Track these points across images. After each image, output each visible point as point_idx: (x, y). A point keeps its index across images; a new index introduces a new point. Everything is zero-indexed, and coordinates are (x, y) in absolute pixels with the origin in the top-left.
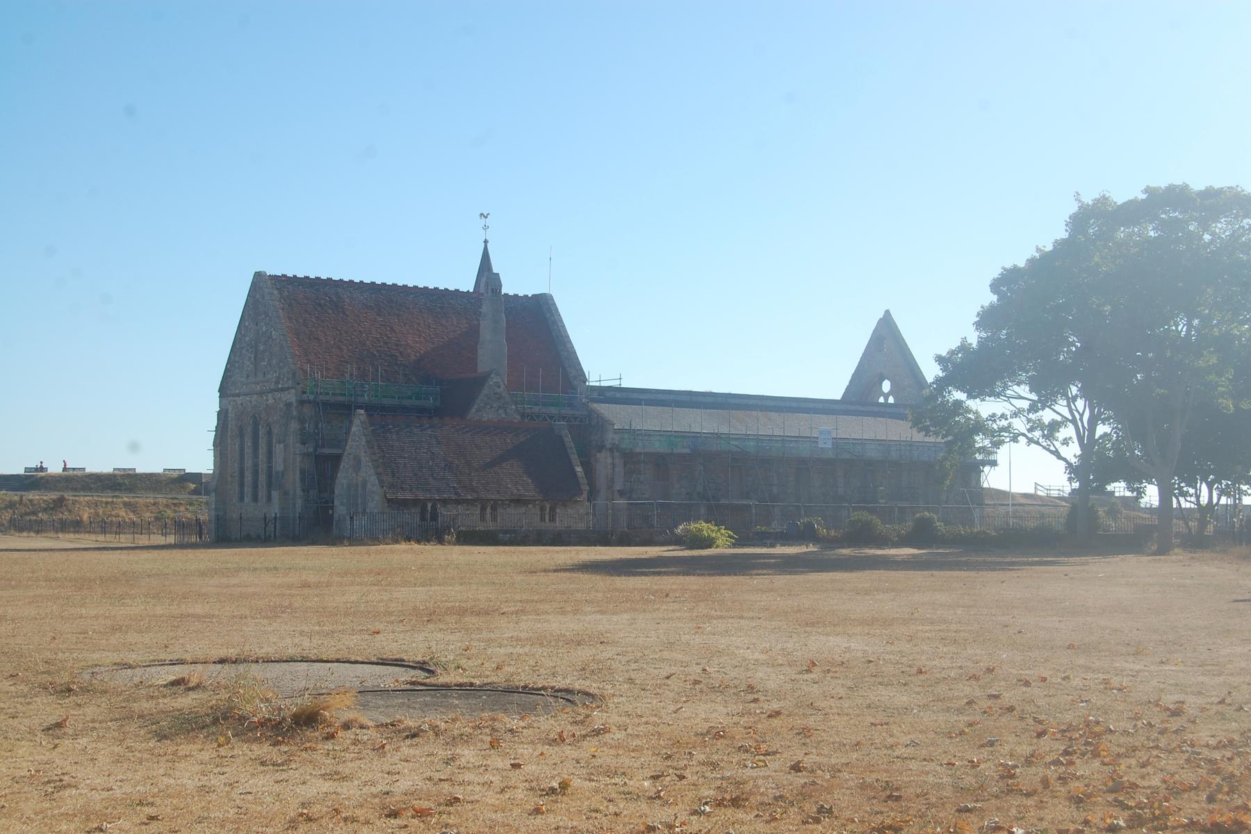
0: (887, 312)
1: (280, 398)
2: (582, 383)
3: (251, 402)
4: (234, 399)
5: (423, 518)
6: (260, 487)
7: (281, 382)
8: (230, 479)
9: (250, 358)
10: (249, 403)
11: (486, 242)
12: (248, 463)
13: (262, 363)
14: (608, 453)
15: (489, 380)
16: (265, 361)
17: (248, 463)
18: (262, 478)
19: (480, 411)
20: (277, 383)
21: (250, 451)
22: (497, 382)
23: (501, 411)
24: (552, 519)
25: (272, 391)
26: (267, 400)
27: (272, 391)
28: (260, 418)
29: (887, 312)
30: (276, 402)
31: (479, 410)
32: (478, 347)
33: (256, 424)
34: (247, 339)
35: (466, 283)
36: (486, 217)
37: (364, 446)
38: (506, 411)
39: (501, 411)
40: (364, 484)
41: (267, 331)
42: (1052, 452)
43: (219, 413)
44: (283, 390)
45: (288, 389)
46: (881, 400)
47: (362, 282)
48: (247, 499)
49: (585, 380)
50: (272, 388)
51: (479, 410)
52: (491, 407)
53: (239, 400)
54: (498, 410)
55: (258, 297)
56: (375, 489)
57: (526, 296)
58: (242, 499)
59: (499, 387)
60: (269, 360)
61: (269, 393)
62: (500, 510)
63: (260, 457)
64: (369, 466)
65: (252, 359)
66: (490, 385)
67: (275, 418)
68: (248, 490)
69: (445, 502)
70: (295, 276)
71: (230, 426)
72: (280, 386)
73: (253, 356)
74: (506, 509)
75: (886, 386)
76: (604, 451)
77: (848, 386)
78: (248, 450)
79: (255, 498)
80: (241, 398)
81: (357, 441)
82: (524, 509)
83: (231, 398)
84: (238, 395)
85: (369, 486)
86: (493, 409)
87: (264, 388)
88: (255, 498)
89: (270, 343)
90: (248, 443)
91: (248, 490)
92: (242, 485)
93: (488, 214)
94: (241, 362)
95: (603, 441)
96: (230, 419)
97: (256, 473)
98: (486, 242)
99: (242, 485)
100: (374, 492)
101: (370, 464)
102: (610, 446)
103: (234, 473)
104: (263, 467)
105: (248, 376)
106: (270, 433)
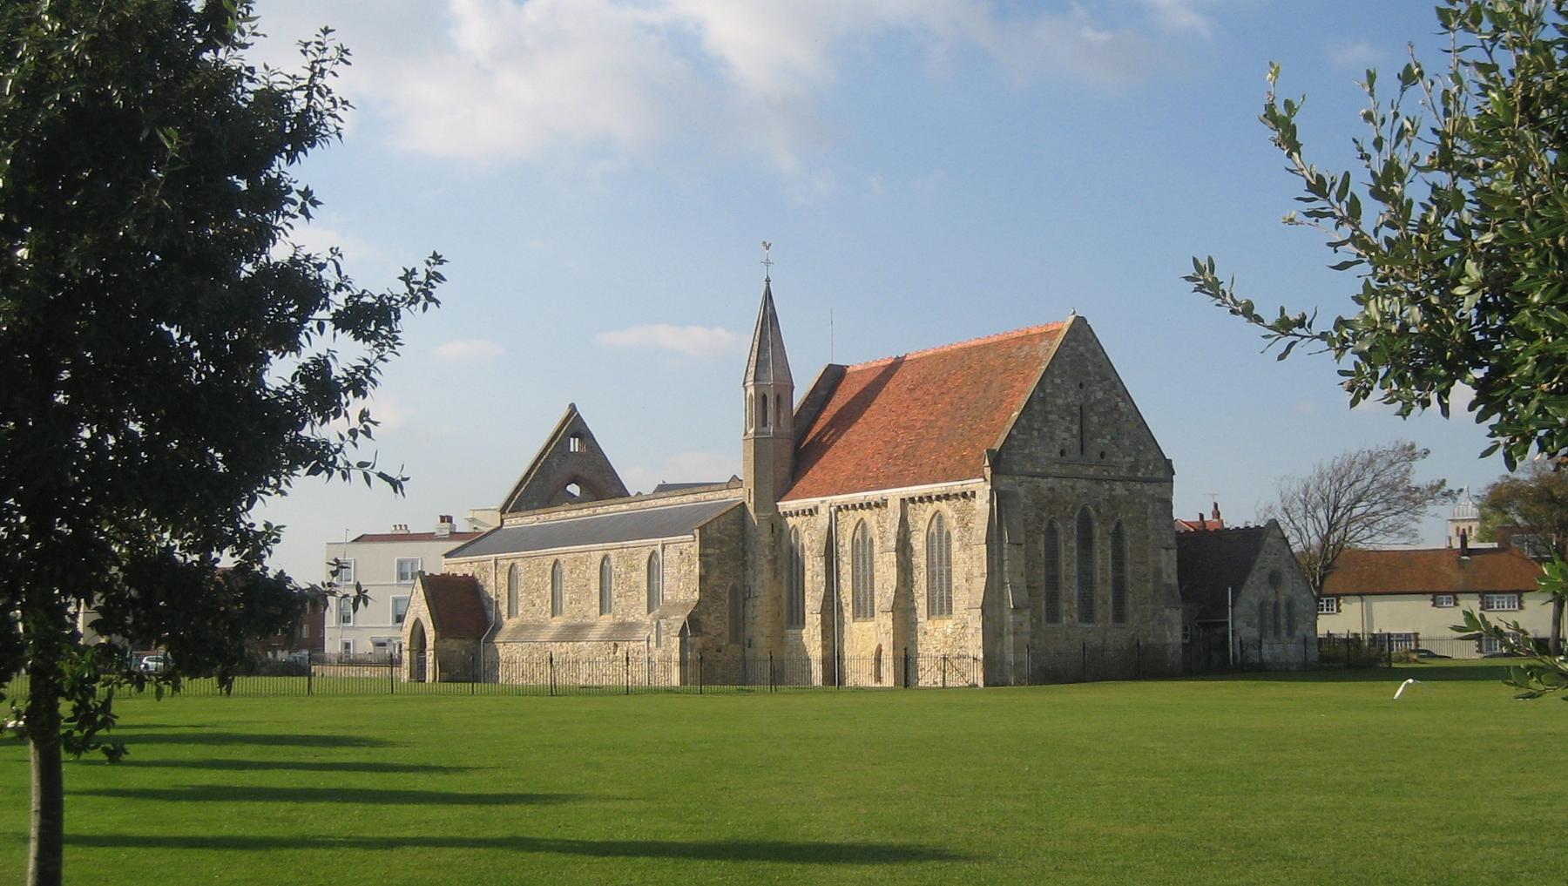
0: (573, 408)
3: (1073, 488)
4: (1030, 479)
7: (1143, 470)
10: (1070, 490)
11: (768, 281)
13: (1099, 440)
16: (1103, 437)
18: (1104, 592)
20: (1134, 467)
25: (1122, 479)
26: (1111, 489)
27: (1122, 479)
29: (573, 408)
40: (1290, 604)
50: (1122, 474)
53: (1044, 484)
61: (1116, 481)
65: (1075, 432)
67: (1130, 515)
72: (1140, 475)
73: (1075, 428)
80: (1050, 480)
83: (1023, 478)
84: (1044, 476)
87: (1105, 473)
88: (1087, 614)
94: (1045, 430)
97: (1086, 581)
98: (768, 281)
99: (1053, 598)
100: (1307, 612)
105: (1062, 453)
106: (1118, 535)
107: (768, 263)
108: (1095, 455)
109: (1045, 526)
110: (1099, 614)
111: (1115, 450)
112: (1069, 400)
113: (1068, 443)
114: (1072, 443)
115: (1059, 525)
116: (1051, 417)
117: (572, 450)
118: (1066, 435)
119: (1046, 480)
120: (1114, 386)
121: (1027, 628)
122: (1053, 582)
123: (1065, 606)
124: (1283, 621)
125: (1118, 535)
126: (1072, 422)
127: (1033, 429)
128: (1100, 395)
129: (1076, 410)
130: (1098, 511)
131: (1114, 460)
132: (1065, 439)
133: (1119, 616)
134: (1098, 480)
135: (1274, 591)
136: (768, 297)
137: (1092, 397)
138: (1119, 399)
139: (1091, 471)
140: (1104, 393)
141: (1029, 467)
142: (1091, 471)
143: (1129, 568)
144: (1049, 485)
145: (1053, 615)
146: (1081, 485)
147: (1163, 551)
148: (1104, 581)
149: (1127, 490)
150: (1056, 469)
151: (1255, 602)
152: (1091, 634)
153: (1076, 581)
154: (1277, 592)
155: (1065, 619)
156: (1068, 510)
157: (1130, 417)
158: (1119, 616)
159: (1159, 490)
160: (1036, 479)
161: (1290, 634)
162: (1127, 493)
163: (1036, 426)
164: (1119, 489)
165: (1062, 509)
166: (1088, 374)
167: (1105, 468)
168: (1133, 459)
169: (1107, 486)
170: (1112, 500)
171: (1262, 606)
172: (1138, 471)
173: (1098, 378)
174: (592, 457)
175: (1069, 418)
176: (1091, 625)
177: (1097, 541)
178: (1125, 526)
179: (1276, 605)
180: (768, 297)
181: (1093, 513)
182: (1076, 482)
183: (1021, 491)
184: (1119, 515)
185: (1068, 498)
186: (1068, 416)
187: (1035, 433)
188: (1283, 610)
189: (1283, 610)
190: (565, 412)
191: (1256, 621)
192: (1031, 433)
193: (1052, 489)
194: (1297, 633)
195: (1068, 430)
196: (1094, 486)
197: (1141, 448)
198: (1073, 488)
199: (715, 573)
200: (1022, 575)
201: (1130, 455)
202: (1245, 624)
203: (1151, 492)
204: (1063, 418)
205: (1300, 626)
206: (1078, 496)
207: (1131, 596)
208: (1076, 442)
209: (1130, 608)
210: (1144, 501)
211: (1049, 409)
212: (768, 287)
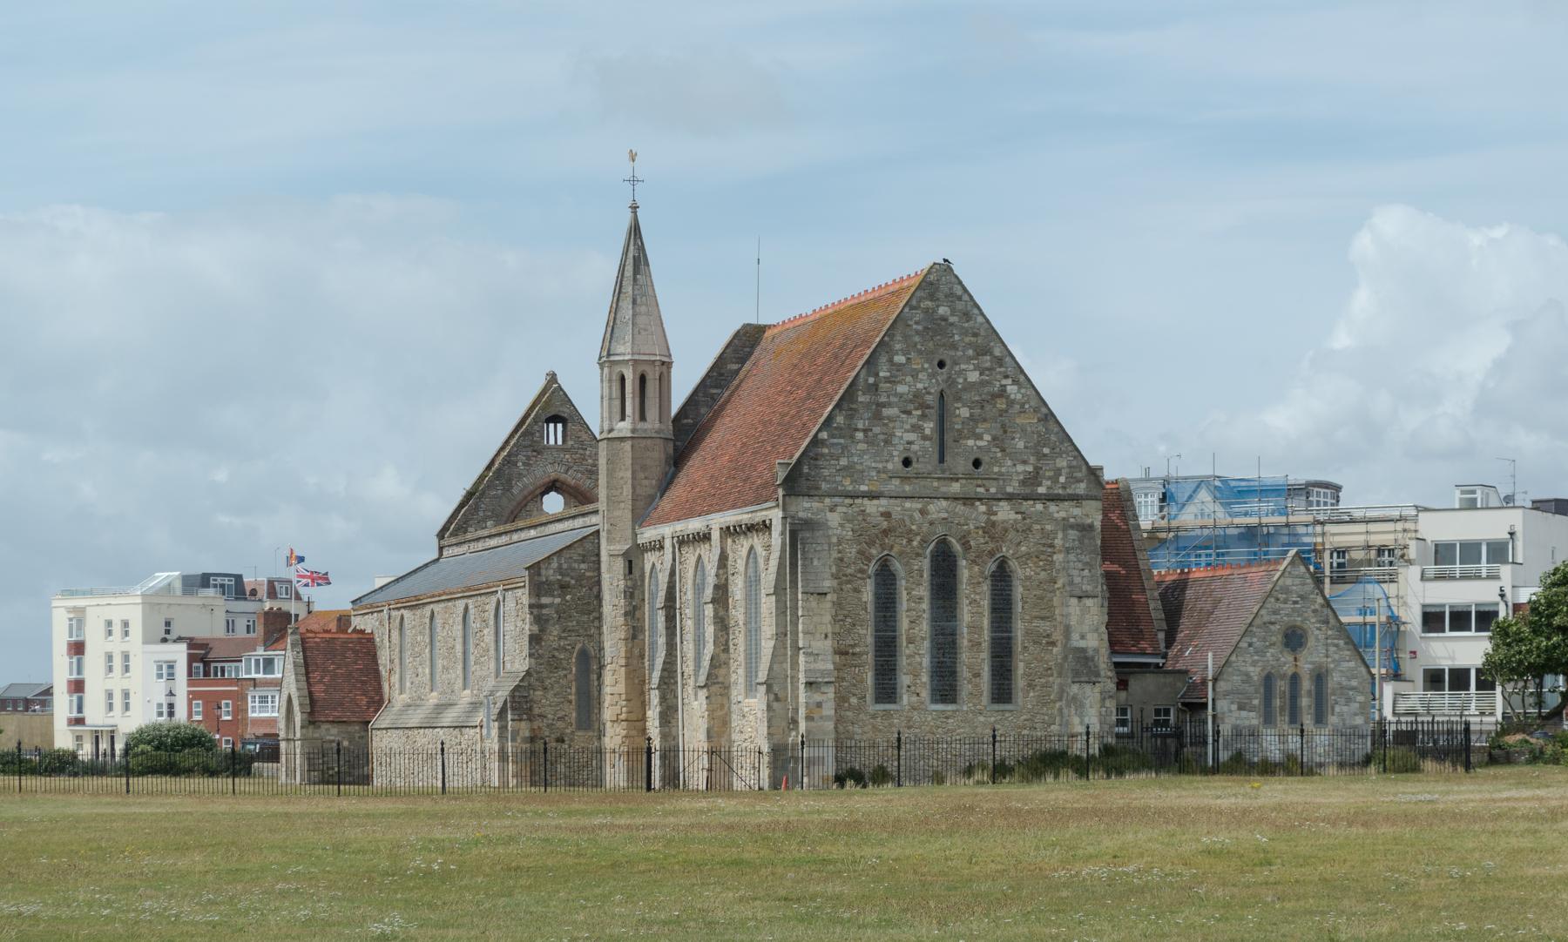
0: (552, 378)
4: (848, 501)
10: (917, 515)
11: (634, 208)
13: (970, 442)
16: (979, 437)
18: (974, 661)
20: (1033, 479)
21: (925, 605)
25: (1010, 498)
26: (991, 512)
28: (966, 546)
29: (552, 378)
30: (1024, 519)
34: (901, 389)
37: (1315, 611)
40: (1320, 678)
45: (1076, 498)
50: (1009, 490)
53: (872, 507)
56: (1354, 683)
60: (994, 438)
61: (1000, 500)
64: (1336, 646)
65: (928, 432)
72: (1041, 490)
73: (929, 427)
80: (883, 501)
81: (1295, 602)
83: (837, 500)
84: (873, 496)
85: (1335, 679)
98: (634, 208)
100: (1353, 688)
103: (853, 646)
105: (907, 462)
106: (1001, 578)
107: (634, 181)
108: (962, 465)
109: (872, 569)
110: (965, 688)
111: (999, 455)
112: (920, 386)
113: (915, 447)
114: (924, 448)
115: (897, 566)
116: (886, 412)
117: (552, 442)
118: (912, 436)
119: (875, 502)
120: (1000, 361)
121: (829, 710)
122: (886, 648)
123: (904, 680)
124: (1305, 702)
125: (1001, 578)
126: (923, 417)
127: (857, 430)
128: (974, 377)
129: (931, 399)
130: (966, 546)
131: (996, 469)
132: (909, 443)
133: (1002, 692)
134: (968, 500)
135: (1291, 659)
136: (635, 231)
137: (961, 380)
138: (1009, 381)
139: (955, 487)
140: (981, 375)
141: (848, 485)
142: (955, 487)
143: (1019, 628)
144: (881, 509)
145: (886, 691)
146: (938, 509)
147: (1074, 601)
148: (976, 645)
149: (1017, 513)
151: (1255, 672)
152: (950, 721)
153: (927, 644)
154: (1296, 659)
155: (905, 699)
156: (915, 543)
157: (1027, 406)
158: (1002, 692)
159: (1077, 511)
160: (858, 501)
161: (1320, 719)
162: (1019, 517)
163: (860, 426)
164: (1005, 512)
165: (904, 542)
166: (954, 347)
167: (979, 482)
168: (1030, 468)
169: (983, 508)
170: (990, 529)
171: (1268, 680)
172: (1040, 484)
173: (970, 352)
174: (581, 451)
175: (919, 412)
176: (950, 707)
177: (964, 587)
178: (1013, 564)
179: (1295, 679)
180: (635, 231)
181: (957, 547)
182: (929, 503)
183: (834, 519)
184: (1004, 549)
185: (914, 527)
186: (916, 409)
187: (860, 435)
188: (1306, 685)
189: (1306, 685)
190: (539, 384)
191: (1256, 702)
192: (852, 437)
193: (887, 515)
194: (1333, 720)
195: (915, 428)
196: (960, 508)
197: (1046, 451)
198: (923, 512)
199: (555, 631)
200: (826, 636)
201: (1025, 462)
202: (1234, 707)
203: (1063, 514)
204: (909, 413)
205: (1337, 709)
206: (931, 523)
207: (1021, 665)
208: (931, 447)
209: (1020, 682)
210: (1048, 527)
211: (883, 399)
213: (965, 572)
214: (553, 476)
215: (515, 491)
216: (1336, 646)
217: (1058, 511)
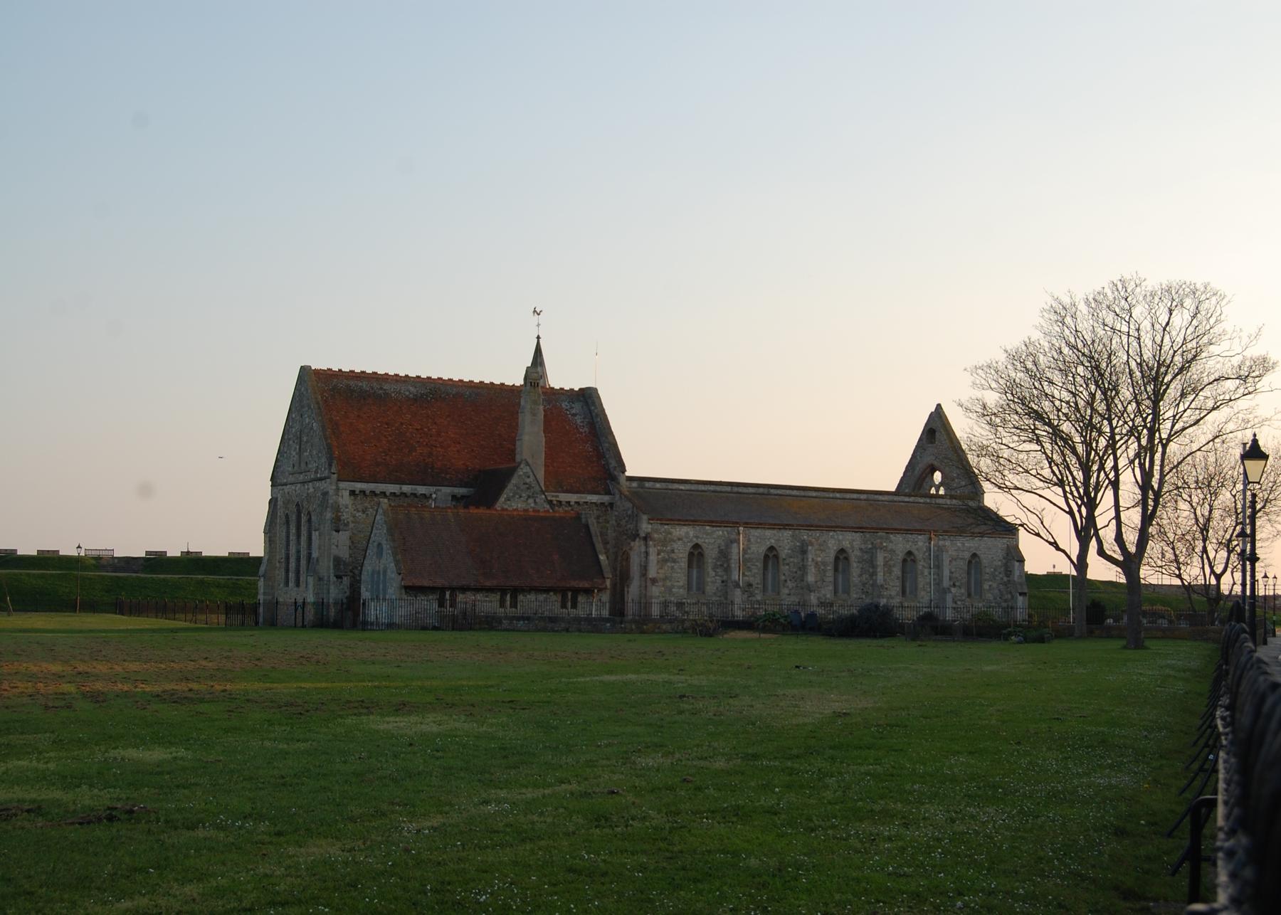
0: (939, 406)
1: (319, 487)
2: (621, 474)
5: (441, 604)
6: (301, 572)
7: (319, 471)
8: (278, 565)
9: (296, 448)
11: (538, 338)
12: (293, 550)
13: (305, 454)
14: (642, 542)
15: (519, 470)
16: (306, 452)
17: (293, 550)
19: (509, 500)
20: (316, 472)
22: (527, 473)
23: (531, 501)
24: (574, 606)
25: (312, 481)
26: (308, 489)
27: (312, 481)
28: (302, 506)
29: (939, 406)
31: (508, 499)
32: (517, 438)
33: (299, 513)
34: (294, 430)
35: (515, 378)
36: (539, 314)
38: (535, 500)
39: (531, 501)
40: (385, 572)
41: (309, 423)
42: (1050, 543)
43: (270, 502)
44: (321, 479)
46: (933, 491)
47: (407, 376)
48: (291, 584)
49: (624, 470)
50: (312, 476)
51: (508, 499)
52: (521, 497)
53: (287, 488)
54: (527, 499)
55: (303, 389)
57: (572, 390)
58: (287, 584)
59: (529, 477)
61: (309, 482)
62: (521, 597)
63: (302, 544)
66: (520, 475)
68: (292, 575)
69: (464, 589)
70: (340, 370)
71: (279, 514)
72: (319, 475)
73: (298, 447)
74: (526, 596)
75: (938, 476)
76: (638, 540)
77: (902, 478)
78: (293, 538)
79: (298, 584)
80: (288, 487)
82: (545, 596)
84: (286, 484)
85: (389, 572)
86: (522, 499)
88: (298, 584)
89: (312, 434)
90: (293, 530)
91: (292, 575)
92: (287, 571)
93: (541, 311)
95: (638, 531)
96: (279, 507)
98: (538, 338)
99: (287, 571)
101: (390, 552)
102: (644, 535)
104: (304, 553)
108: (303, 465)
132: (294, 457)
142: (301, 477)
150: (291, 479)
159: (325, 485)
171: (373, 572)
212: (538, 344)
213: (304, 519)
214: (930, 462)
215: (916, 472)
216: (389, 553)
217: (323, 485)
